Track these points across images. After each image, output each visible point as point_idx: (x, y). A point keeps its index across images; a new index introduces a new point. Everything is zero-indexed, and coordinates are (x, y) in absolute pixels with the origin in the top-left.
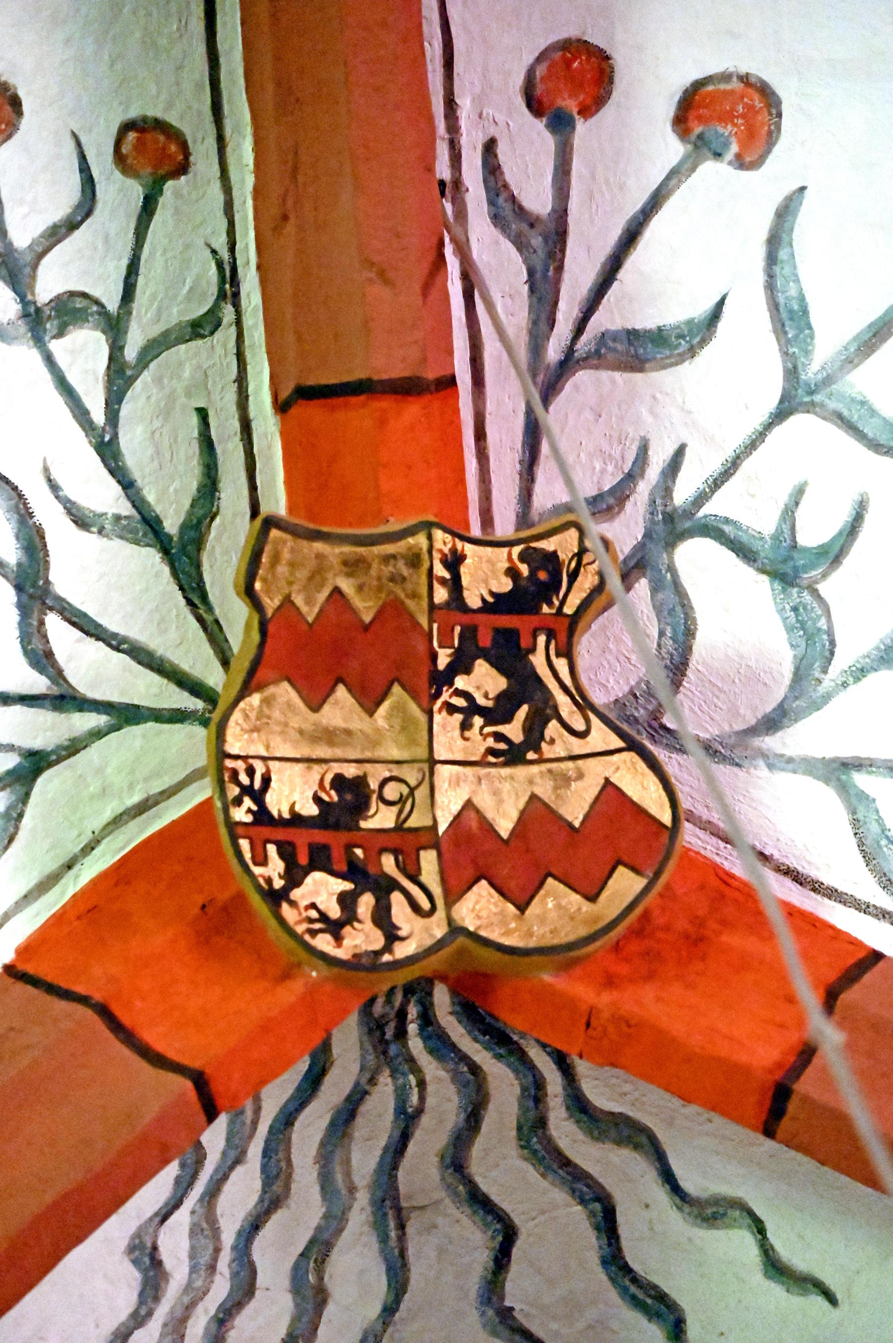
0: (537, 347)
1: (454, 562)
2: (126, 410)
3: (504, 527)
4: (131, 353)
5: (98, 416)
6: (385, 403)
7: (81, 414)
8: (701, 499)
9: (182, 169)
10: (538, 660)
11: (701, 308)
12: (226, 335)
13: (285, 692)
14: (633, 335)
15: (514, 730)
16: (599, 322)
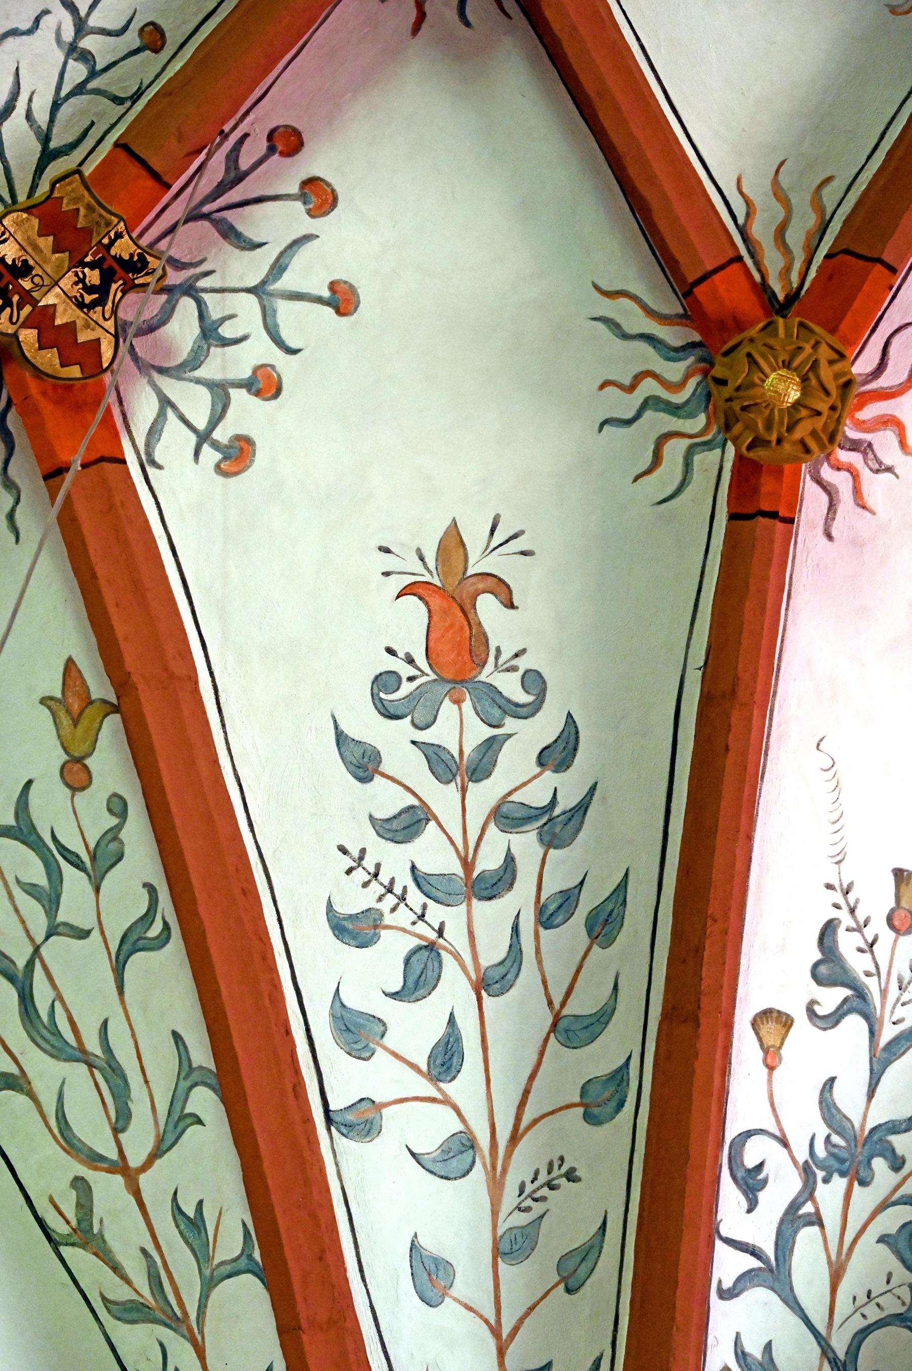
0: (203, 203)
1: (119, 236)
2: (72, 100)
3: (144, 242)
4: (90, 86)
5: (63, 93)
6: (144, 173)
7: (59, 88)
8: (205, 290)
9: (156, 51)
10: (114, 286)
11: (257, 239)
12: (121, 109)
13: (35, 222)
14: (232, 228)
15: (88, 299)
16: (227, 214)
